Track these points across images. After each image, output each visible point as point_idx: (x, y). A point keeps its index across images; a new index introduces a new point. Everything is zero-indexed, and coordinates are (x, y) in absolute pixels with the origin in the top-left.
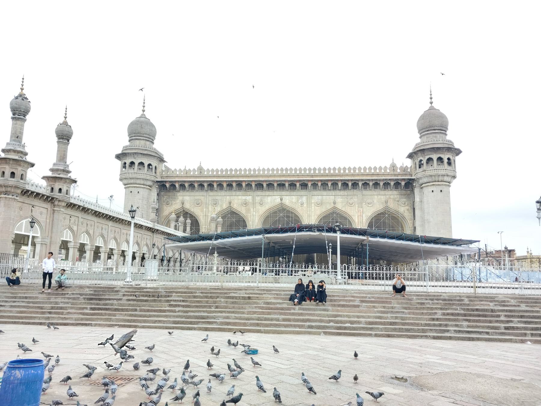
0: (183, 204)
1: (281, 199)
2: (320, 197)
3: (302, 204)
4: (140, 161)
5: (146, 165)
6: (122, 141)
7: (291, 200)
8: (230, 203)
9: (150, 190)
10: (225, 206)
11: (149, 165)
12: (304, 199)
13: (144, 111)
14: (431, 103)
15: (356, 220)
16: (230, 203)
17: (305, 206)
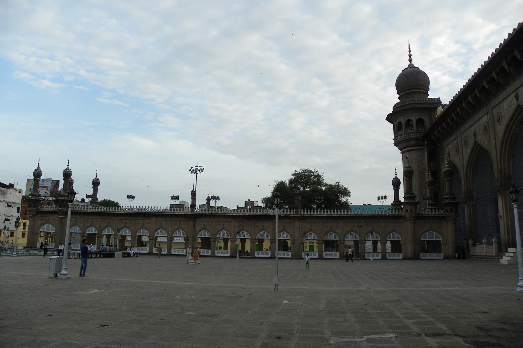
8: (475, 135)
9: (422, 149)
11: (409, 121)
13: (410, 60)
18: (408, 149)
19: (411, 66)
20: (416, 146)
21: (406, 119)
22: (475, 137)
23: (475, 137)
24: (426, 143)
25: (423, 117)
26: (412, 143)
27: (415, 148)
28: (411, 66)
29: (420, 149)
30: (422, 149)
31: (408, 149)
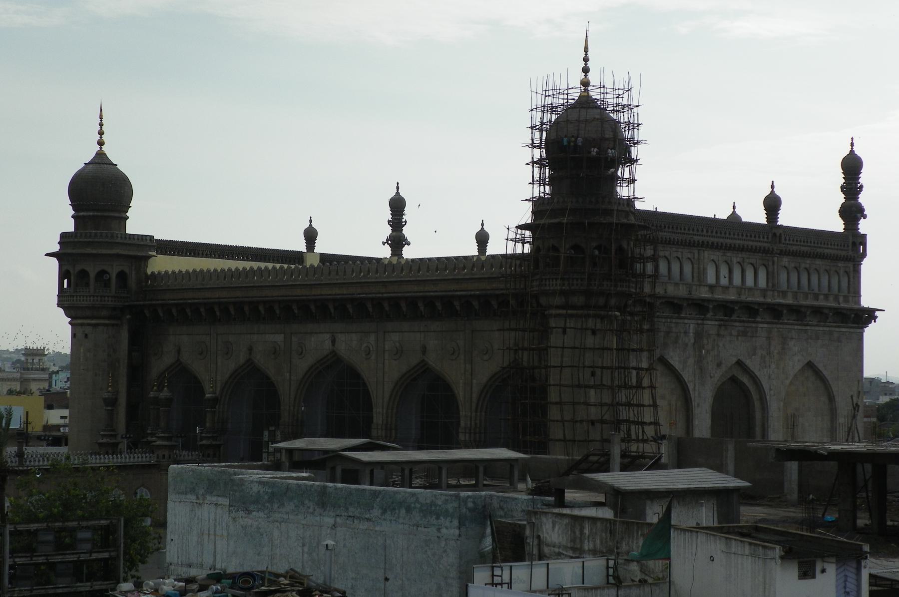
0: (179, 351)
1: (333, 342)
2: (395, 337)
3: (368, 353)
4: (78, 268)
5: (92, 275)
6: (64, 220)
7: (349, 342)
8: (250, 350)
10: (242, 360)
12: (372, 338)
13: (101, 143)
14: (585, 84)
15: (461, 394)
16: (250, 350)
17: (373, 357)
18: (93, 322)
19: (101, 157)
20: (109, 318)
21: (98, 269)
22: (250, 354)
23: (250, 354)
24: (128, 317)
25: (127, 270)
26: (104, 313)
27: (107, 322)
28: (101, 157)
29: (113, 325)
30: (117, 325)
31: (93, 322)
